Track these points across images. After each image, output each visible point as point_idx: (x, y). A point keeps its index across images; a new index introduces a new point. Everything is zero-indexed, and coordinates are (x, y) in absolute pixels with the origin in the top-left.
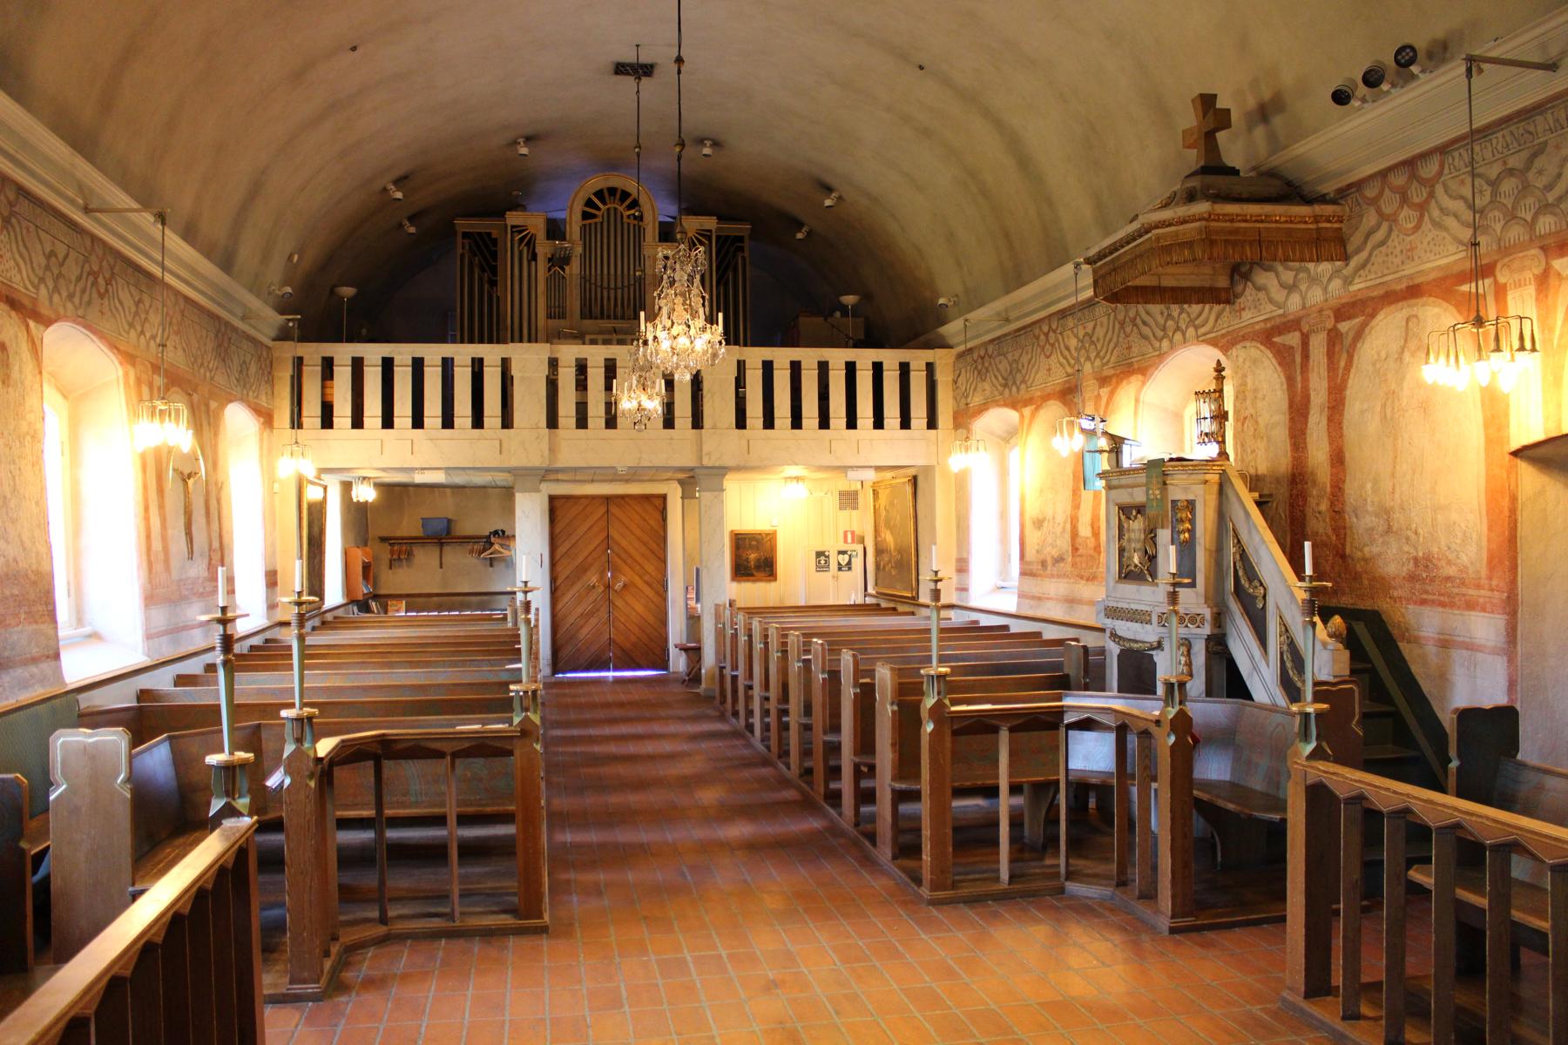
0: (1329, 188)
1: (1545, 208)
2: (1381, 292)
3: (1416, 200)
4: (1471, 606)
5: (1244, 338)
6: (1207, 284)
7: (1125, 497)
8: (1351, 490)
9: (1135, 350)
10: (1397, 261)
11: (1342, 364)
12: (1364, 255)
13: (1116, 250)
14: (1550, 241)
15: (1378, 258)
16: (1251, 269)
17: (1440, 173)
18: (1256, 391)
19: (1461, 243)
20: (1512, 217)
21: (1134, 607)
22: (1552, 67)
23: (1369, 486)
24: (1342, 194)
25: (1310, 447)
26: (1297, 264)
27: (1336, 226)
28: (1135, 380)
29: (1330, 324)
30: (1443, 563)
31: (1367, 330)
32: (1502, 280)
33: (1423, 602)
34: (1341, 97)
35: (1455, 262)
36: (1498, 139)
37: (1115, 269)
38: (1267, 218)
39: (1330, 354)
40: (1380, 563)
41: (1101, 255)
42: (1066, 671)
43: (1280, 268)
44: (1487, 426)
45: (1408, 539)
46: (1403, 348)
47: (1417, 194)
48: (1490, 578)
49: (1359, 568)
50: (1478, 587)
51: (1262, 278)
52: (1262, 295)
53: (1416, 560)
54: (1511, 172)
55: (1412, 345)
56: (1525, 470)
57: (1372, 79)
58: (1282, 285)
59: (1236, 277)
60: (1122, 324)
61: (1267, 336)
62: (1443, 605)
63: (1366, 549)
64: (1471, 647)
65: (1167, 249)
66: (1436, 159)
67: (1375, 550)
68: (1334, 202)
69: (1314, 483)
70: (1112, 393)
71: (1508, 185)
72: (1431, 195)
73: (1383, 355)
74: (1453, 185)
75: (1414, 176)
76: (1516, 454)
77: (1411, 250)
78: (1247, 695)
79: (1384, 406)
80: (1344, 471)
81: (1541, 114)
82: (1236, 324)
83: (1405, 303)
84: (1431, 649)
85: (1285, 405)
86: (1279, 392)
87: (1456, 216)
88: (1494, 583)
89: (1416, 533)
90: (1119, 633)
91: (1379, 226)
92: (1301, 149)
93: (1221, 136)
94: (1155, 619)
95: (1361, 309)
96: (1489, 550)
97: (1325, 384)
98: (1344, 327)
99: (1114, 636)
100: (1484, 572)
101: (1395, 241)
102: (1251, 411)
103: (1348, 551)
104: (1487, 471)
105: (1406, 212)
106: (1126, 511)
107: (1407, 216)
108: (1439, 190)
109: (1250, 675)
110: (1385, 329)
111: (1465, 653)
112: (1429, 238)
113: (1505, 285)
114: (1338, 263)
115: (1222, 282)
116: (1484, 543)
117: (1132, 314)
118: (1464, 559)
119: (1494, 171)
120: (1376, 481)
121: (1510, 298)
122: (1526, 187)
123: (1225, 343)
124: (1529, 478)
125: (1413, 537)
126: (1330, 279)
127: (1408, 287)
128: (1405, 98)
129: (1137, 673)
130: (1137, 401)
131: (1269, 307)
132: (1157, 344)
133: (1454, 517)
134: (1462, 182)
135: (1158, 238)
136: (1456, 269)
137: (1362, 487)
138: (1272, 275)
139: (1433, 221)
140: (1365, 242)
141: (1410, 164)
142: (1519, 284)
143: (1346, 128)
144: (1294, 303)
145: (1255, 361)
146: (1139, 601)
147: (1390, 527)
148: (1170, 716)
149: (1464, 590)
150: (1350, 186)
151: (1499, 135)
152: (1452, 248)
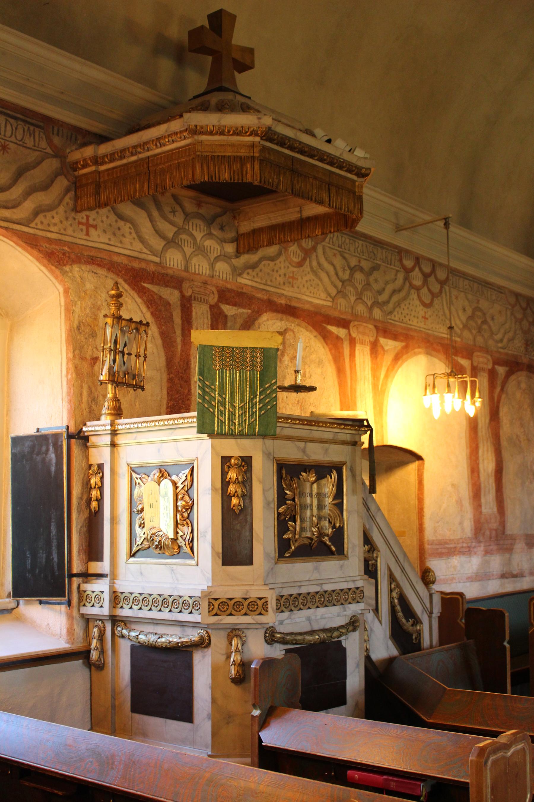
1: (376, 303)
7: (291, 452)
10: (281, 280)
13: (312, 156)
14: (379, 325)
43: (155, 214)
54: (361, 269)
71: (359, 276)
74: (329, 253)
81: (381, 247)
82: (78, 237)
87: (327, 273)
134: (335, 255)
142: (362, 343)
144: (174, 260)
151: (361, 242)
152: (323, 295)
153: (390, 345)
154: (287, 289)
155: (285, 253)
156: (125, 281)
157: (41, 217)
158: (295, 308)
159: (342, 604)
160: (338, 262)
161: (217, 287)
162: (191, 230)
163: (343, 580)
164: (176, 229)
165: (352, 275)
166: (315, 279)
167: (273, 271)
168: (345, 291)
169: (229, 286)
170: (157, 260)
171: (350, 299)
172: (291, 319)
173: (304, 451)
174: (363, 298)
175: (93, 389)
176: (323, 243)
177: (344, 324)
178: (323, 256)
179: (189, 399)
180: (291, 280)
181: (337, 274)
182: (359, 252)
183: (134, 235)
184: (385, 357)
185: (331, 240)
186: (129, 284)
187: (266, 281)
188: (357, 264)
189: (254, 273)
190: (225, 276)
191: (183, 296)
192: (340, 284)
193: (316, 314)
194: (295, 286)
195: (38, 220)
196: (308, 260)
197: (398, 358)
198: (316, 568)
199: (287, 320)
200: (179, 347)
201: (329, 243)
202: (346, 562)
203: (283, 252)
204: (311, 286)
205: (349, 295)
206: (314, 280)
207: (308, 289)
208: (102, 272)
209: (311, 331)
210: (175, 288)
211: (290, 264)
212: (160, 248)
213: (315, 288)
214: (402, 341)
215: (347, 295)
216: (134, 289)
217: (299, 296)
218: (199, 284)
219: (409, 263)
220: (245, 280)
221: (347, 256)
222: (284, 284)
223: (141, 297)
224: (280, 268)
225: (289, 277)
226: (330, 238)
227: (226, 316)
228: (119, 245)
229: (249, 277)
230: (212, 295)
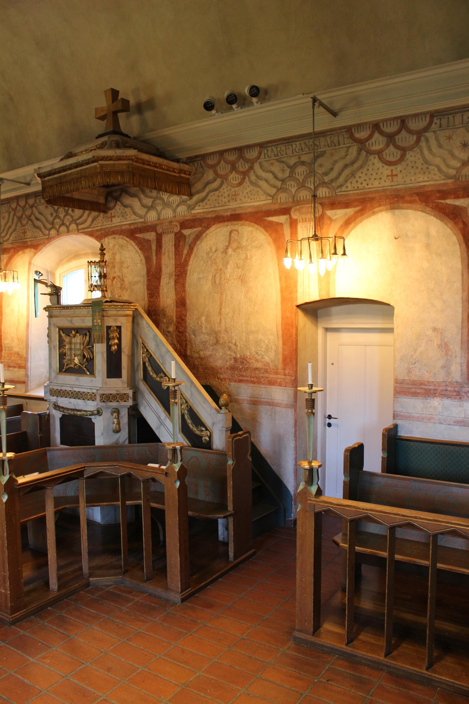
0: (183, 156)
1: (323, 184)
2: (214, 215)
3: (241, 169)
4: (271, 383)
5: (114, 233)
6: (95, 200)
7: (65, 323)
8: (191, 322)
9: (29, 234)
10: (226, 200)
11: (185, 252)
12: (203, 194)
13: (64, 170)
14: (326, 201)
15: (212, 197)
16: (120, 195)
17: (258, 157)
18: (122, 263)
19: (269, 195)
20: (302, 186)
21: (77, 390)
22: (334, 114)
23: (203, 319)
24: (190, 160)
25: (161, 296)
26: (154, 193)
27: (188, 177)
28: (28, 253)
29: (177, 229)
30: (253, 361)
31: (204, 235)
32: (294, 216)
33: (240, 381)
34: (209, 106)
35: (264, 204)
36: (297, 145)
37: (61, 182)
38: (160, 166)
39: (177, 246)
40: (211, 360)
41: (50, 173)
42: (24, 429)
43: (142, 196)
44: (282, 291)
45: (230, 348)
46: (227, 247)
47: (242, 166)
48: (284, 369)
49: (196, 362)
50: (277, 373)
51: (128, 200)
52: (128, 210)
53: (236, 359)
54: (303, 163)
55: (234, 245)
56: (300, 314)
57: (232, 100)
58: (143, 206)
59: (110, 198)
60: (20, 218)
61: (132, 233)
62: (253, 382)
63: (202, 353)
64: (271, 404)
65: (107, 173)
66: (257, 150)
67: (208, 353)
68: (186, 163)
69: (165, 315)
70: (10, 259)
71: (301, 170)
72: (251, 168)
73: (214, 249)
74: (266, 164)
75: (241, 156)
76: (298, 306)
77: (235, 195)
78: (156, 439)
79: (214, 277)
80: (186, 310)
81: (324, 136)
82: (108, 225)
83: (229, 223)
84: (246, 406)
85: (144, 272)
86: (139, 265)
87: (266, 181)
88: (287, 372)
89: (235, 345)
90: (61, 404)
91: (214, 180)
92: (169, 132)
93: (120, 115)
94: (98, 398)
95: (204, 223)
96: (283, 354)
97: (173, 262)
98: (186, 232)
99: (57, 407)
100: (280, 366)
101: (225, 190)
102: (118, 274)
103: (188, 353)
104: (282, 314)
105: (234, 174)
106: (65, 331)
107: (234, 177)
108: (257, 166)
109: (158, 428)
110: (216, 236)
111: (268, 407)
112: (247, 191)
113: (296, 220)
114: (185, 197)
115: (102, 200)
116: (280, 350)
117: (28, 213)
118: (267, 359)
119: (292, 161)
120: (208, 316)
121: (299, 227)
122: (312, 173)
123: (99, 235)
124: (302, 320)
125: (233, 347)
126: (178, 206)
127: (232, 215)
128: (240, 115)
129: (78, 429)
130: (30, 263)
131: (134, 217)
132: (47, 232)
133: (260, 337)
134: (272, 164)
135: (102, 166)
136: (264, 209)
137: (199, 318)
138: (136, 200)
139: (251, 182)
140: (205, 187)
141: (240, 150)
142: (304, 221)
143: (201, 124)
144: (152, 216)
145: (121, 246)
146: (80, 386)
147: (217, 341)
148: (177, 470)
149: (267, 375)
150: (197, 157)
151: (298, 143)
152: (263, 197)
153: (339, 215)
154: (232, 204)
155: (226, 182)
156: (127, 237)
157: (95, 222)
158: (239, 215)
159: (84, 399)
160: (276, 168)
161: (178, 221)
162: (161, 196)
163: (89, 388)
164: (152, 200)
165: (292, 172)
166: (254, 188)
167: (219, 196)
168: (285, 187)
169: (187, 218)
170: (142, 220)
171: (291, 191)
172: (236, 222)
173: (71, 322)
174: (307, 185)
175: (113, 292)
176: (259, 161)
177: (286, 211)
178: (260, 170)
179: (159, 288)
180: (234, 197)
181: (276, 177)
182: (297, 151)
183: (131, 213)
184: (332, 225)
185: (266, 155)
186: (129, 238)
187: (214, 205)
188: (298, 160)
189: (204, 204)
190: (183, 213)
191: (157, 234)
192: (279, 184)
193: (257, 213)
194: (238, 200)
195: (93, 224)
196: (247, 178)
197: (348, 223)
198: (77, 380)
199: (232, 225)
200: (155, 262)
201: (265, 158)
202: (94, 379)
203: (224, 182)
204: (252, 194)
205: (290, 188)
206: (253, 190)
207: (248, 197)
208: (117, 236)
209: (253, 226)
210: (152, 231)
211: (231, 187)
212: (144, 213)
213: (255, 195)
214: (357, 206)
215: (288, 189)
216: (131, 239)
217: (241, 205)
218: (167, 224)
219: (391, 129)
220: (198, 211)
221: (284, 159)
222: (229, 201)
223: (134, 242)
224: (224, 193)
225: (233, 195)
226: (264, 154)
227: (185, 236)
228: (125, 220)
229: (200, 208)
230: (176, 227)
